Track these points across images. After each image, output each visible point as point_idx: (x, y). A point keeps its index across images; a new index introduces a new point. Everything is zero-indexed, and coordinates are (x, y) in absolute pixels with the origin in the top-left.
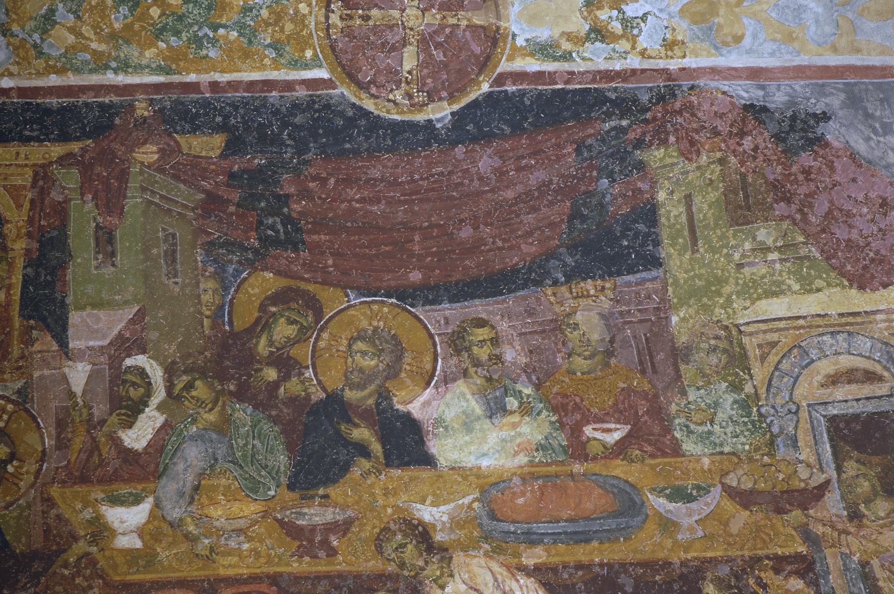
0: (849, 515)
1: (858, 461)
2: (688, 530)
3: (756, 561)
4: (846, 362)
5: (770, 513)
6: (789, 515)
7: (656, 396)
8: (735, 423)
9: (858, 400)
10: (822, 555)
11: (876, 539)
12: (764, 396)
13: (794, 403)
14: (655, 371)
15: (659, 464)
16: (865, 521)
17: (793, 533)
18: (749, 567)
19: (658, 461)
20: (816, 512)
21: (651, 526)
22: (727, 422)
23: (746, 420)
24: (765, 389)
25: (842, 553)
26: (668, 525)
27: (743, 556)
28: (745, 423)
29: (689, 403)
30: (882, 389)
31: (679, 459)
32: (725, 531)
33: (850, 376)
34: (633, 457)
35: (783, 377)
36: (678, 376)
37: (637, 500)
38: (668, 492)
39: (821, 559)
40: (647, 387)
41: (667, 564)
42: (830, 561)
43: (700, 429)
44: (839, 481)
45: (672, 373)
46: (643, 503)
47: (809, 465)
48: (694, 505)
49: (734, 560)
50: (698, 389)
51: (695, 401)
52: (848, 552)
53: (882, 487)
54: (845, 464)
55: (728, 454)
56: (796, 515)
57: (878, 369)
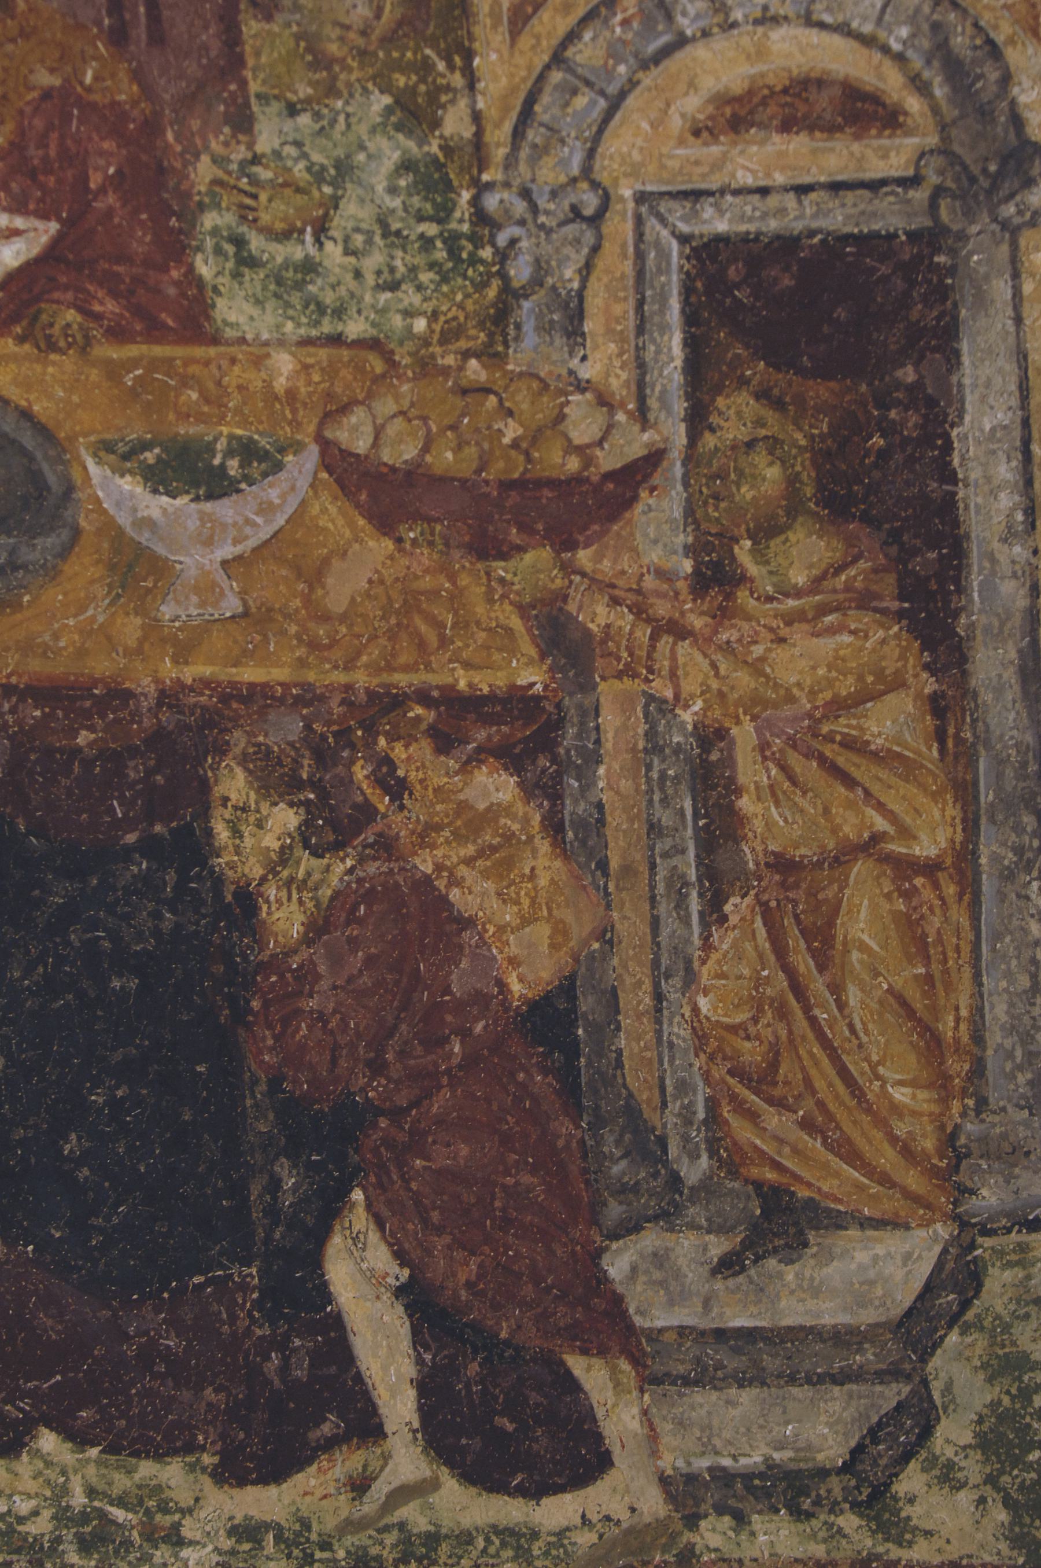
0: (697, 571)
1: (762, 395)
2: (197, 589)
3: (388, 704)
4: (794, 50)
5: (456, 554)
6: (512, 564)
7: (152, 127)
8: (394, 237)
9: (802, 190)
10: (588, 701)
11: (762, 659)
12: (501, 152)
13: (595, 185)
14: (157, 37)
15: (135, 363)
16: (742, 595)
17: (516, 623)
18: (362, 724)
19: (133, 351)
20: (598, 558)
21: (84, 570)
22: (369, 242)
23: (431, 229)
24: (508, 127)
25: (651, 698)
26: (136, 568)
27: (348, 687)
28: (427, 243)
29: (256, 160)
30: (890, 157)
31: (199, 352)
32: (307, 601)
33: (798, 104)
34: (56, 330)
35: (575, 92)
36: (233, 60)
37: (52, 479)
38: (150, 457)
39: (583, 713)
40: (126, 91)
41: (119, 695)
42: (609, 719)
43: (281, 252)
44: (690, 457)
45: (216, 47)
46: (70, 489)
47: (604, 401)
48: (225, 509)
49: (322, 699)
50: (292, 110)
51: (277, 154)
52: (669, 694)
53: (820, 487)
54: (721, 402)
55: (359, 343)
56: (533, 565)
57: (892, 83)
